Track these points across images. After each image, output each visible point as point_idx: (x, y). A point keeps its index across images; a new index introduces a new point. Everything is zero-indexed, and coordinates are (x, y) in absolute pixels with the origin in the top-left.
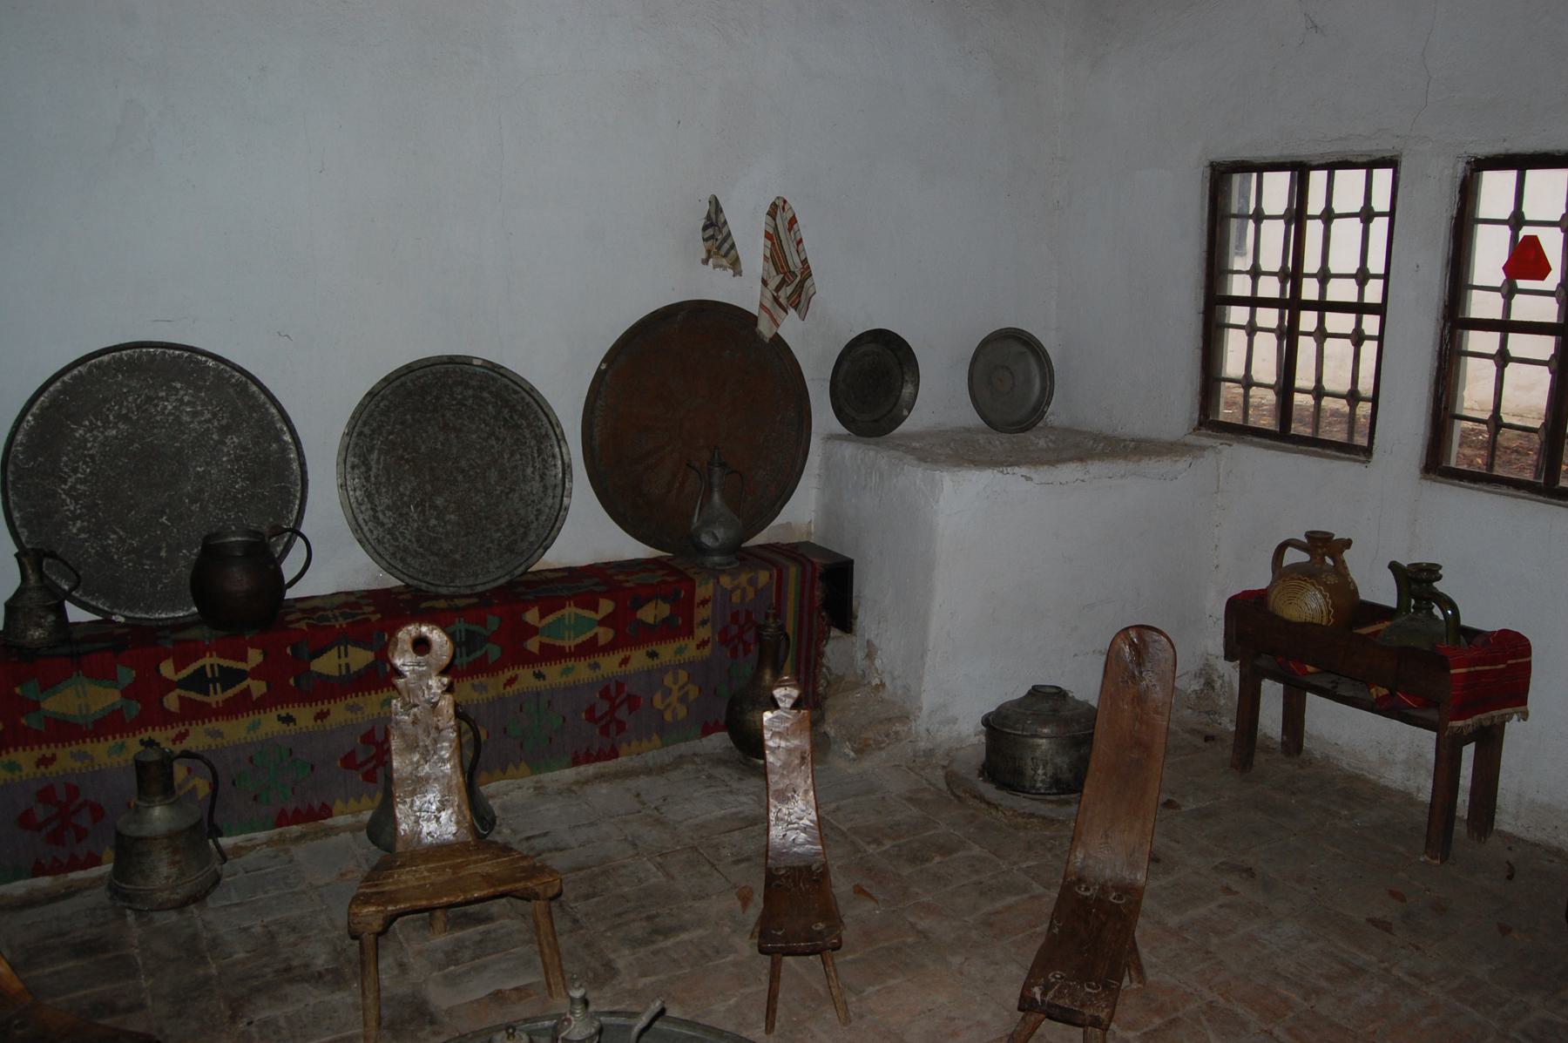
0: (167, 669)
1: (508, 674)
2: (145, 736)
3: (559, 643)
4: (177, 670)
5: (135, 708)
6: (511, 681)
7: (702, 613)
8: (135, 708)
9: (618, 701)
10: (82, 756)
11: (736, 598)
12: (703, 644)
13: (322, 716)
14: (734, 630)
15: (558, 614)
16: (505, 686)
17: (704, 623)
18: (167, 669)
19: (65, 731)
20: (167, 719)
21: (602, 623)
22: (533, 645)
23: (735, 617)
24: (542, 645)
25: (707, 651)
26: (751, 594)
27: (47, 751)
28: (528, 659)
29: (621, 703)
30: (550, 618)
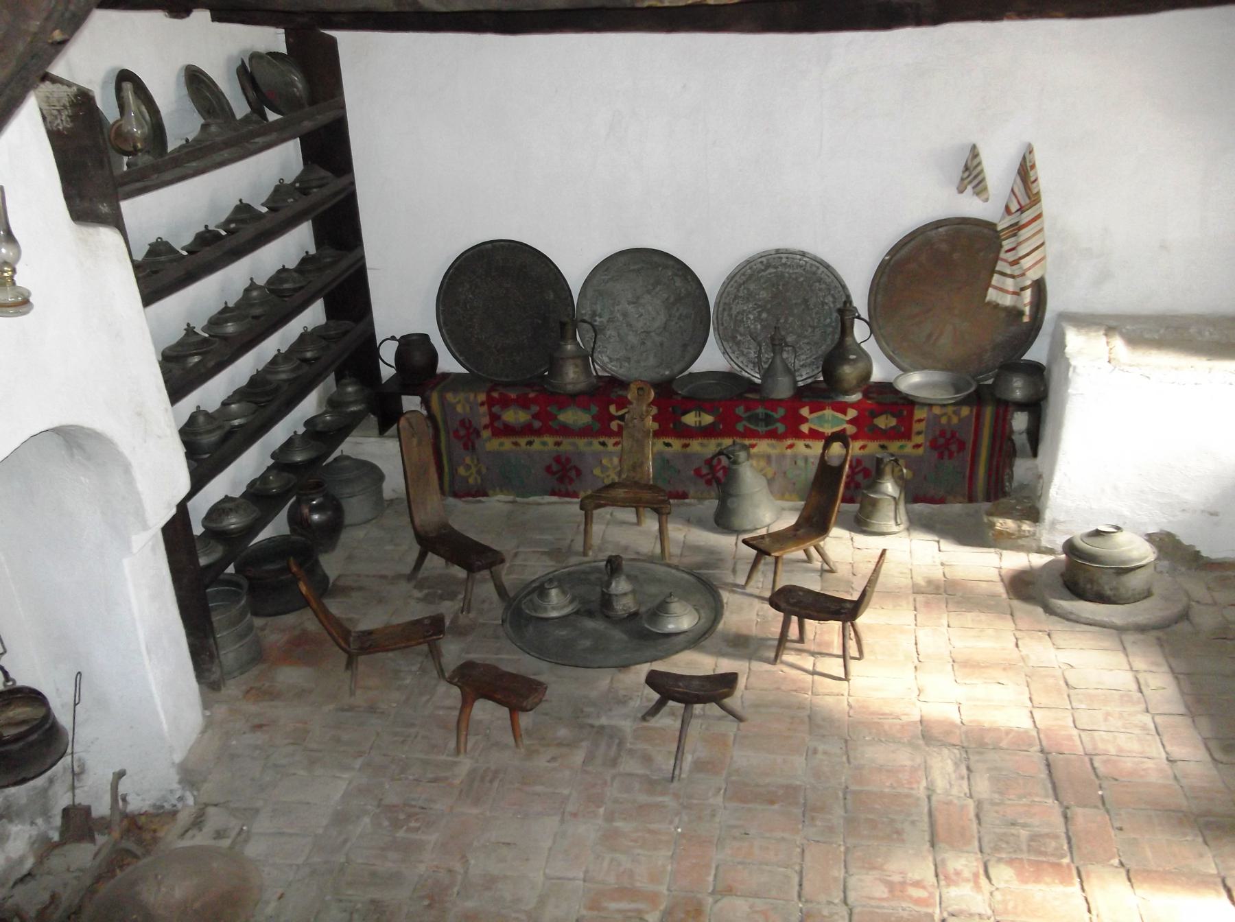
0: (612, 409)
1: (789, 442)
2: (602, 440)
3: (821, 430)
4: (617, 411)
5: (597, 426)
6: (791, 446)
7: (917, 427)
8: (597, 426)
9: (857, 470)
10: (574, 444)
11: (944, 420)
12: (917, 446)
13: (686, 446)
14: (941, 441)
15: (820, 413)
16: (787, 448)
17: (919, 433)
18: (612, 409)
19: (565, 431)
20: (611, 434)
21: (851, 422)
22: (805, 428)
23: (943, 434)
24: (811, 430)
25: (920, 451)
26: (955, 420)
27: (558, 439)
28: (799, 435)
29: (859, 472)
30: (815, 415)
